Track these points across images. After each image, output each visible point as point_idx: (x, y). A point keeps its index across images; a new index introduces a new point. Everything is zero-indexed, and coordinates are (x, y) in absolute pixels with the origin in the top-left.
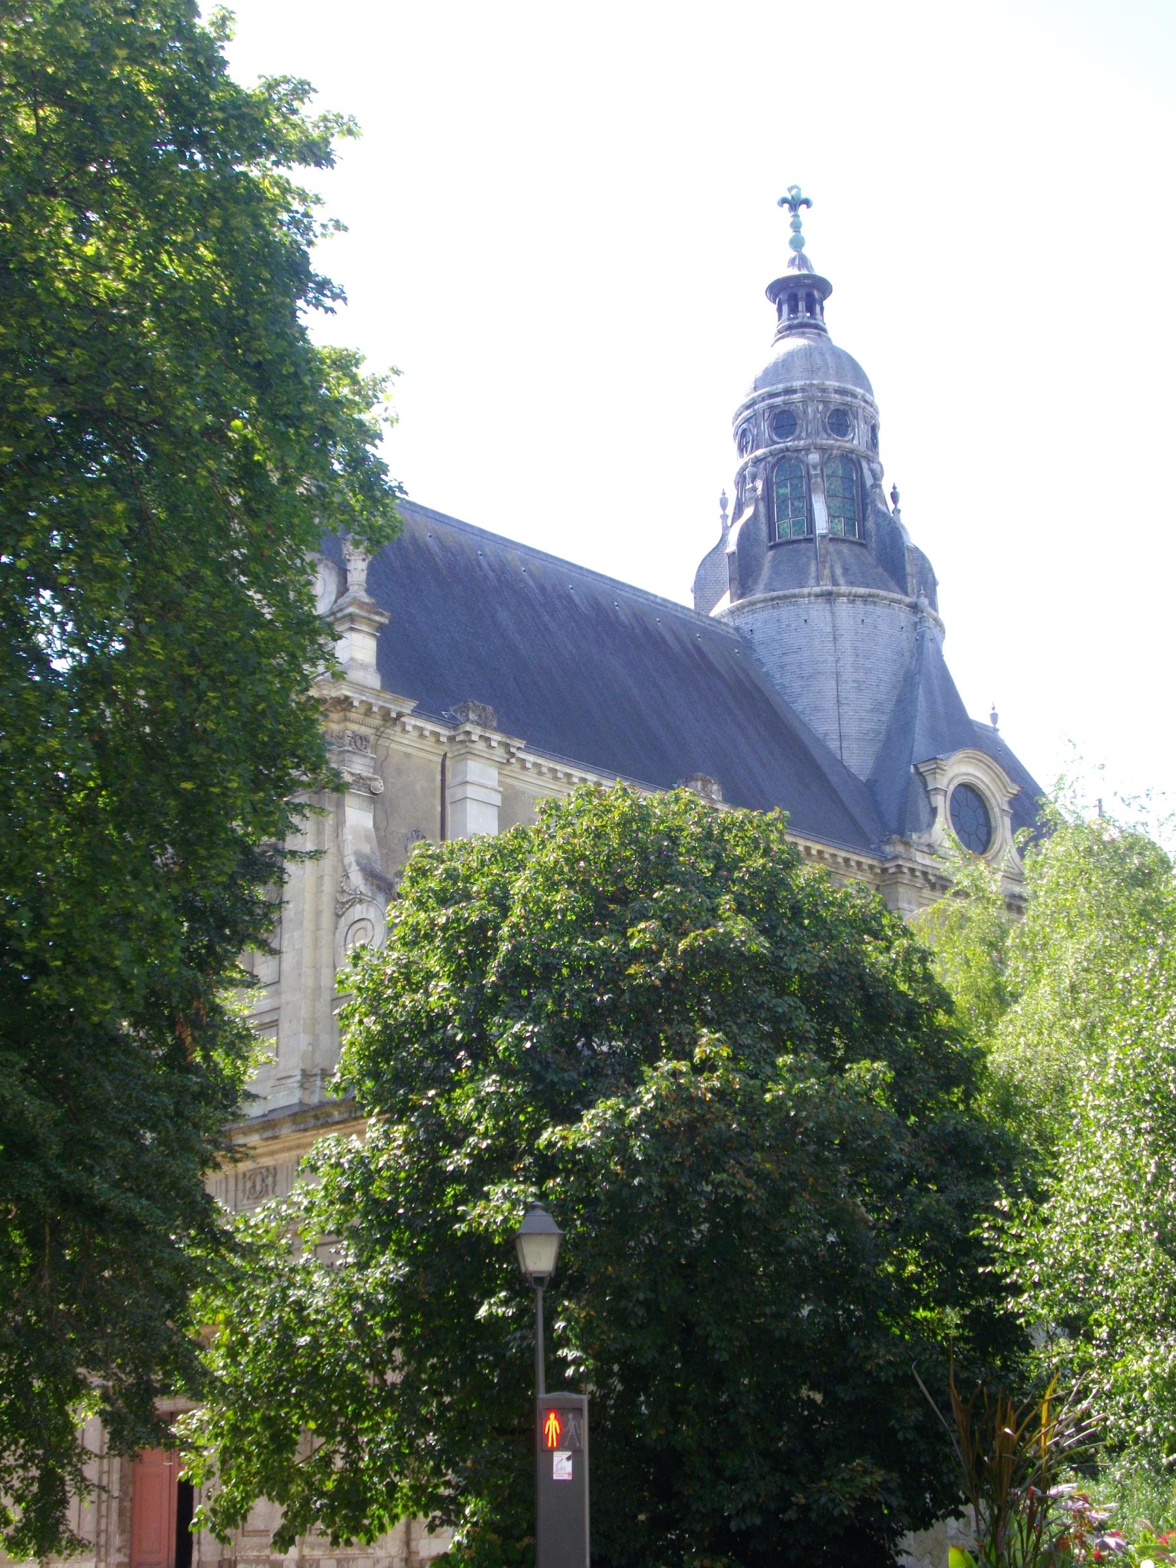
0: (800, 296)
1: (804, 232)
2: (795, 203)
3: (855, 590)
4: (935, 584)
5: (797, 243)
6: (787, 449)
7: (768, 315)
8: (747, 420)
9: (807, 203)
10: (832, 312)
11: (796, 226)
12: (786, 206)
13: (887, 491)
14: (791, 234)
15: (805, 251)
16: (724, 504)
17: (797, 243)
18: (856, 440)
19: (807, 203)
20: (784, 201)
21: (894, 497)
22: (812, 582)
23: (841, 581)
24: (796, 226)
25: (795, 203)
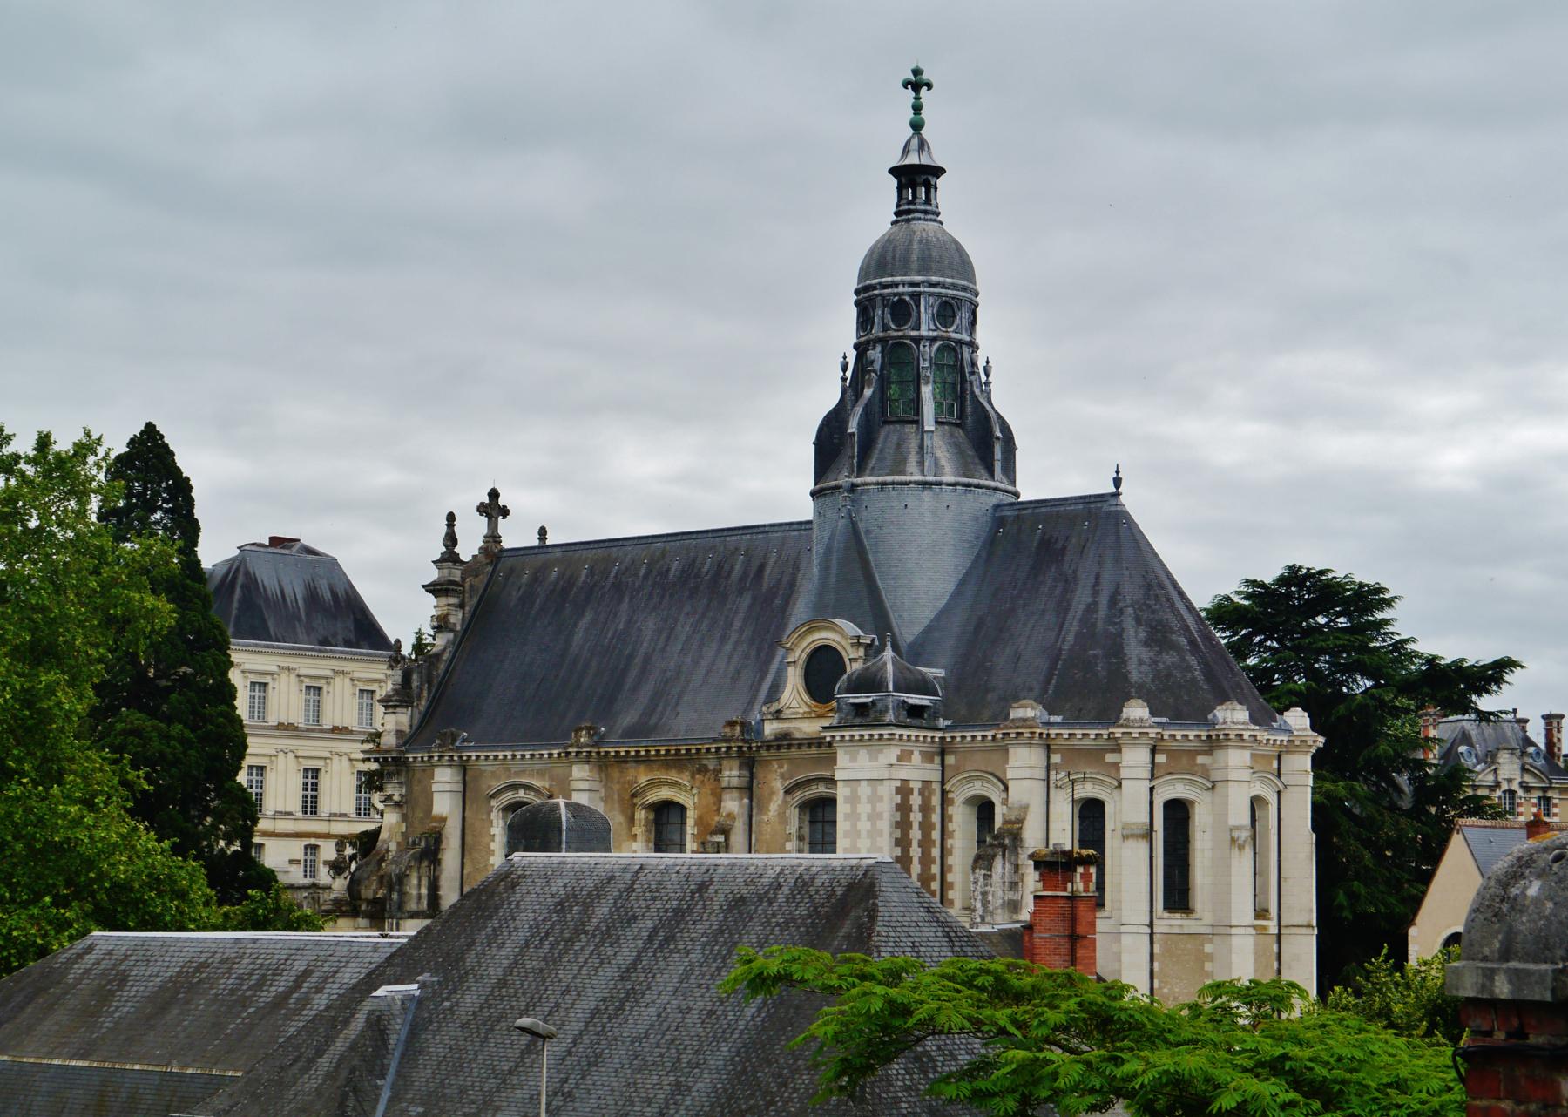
1: (924, 113)
2: (917, 84)
5: (917, 126)
9: (929, 86)
11: (917, 108)
13: (981, 364)
17: (917, 126)
19: (929, 86)
20: (906, 84)
21: (987, 375)
24: (917, 108)
25: (917, 84)
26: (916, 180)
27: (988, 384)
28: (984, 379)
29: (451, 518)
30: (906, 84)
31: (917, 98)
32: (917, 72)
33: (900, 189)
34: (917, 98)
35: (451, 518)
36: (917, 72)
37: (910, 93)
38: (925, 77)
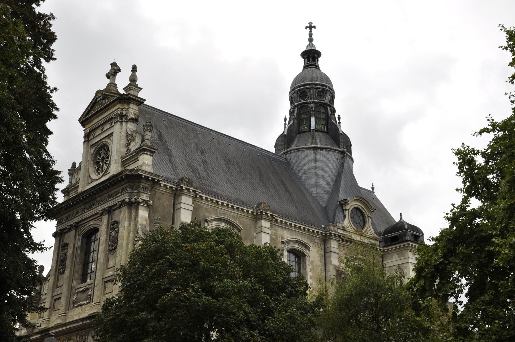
0: (311, 56)
1: (313, 37)
3: (322, 146)
4: (351, 145)
5: (311, 40)
6: (304, 103)
7: (301, 63)
8: (292, 94)
10: (322, 62)
11: (311, 35)
12: (308, 29)
13: (336, 116)
14: (308, 37)
15: (313, 42)
16: (285, 120)
17: (311, 40)
18: (326, 100)
19: (315, 27)
20: (307, 28)
22: (309, 144)
23: (319, 144)
24: (311, 35)
26: (311, 56)
27: (340, 123)
28: (338, 121)
29: (134, 69)
30: (307, 28)
31: (311, 32)
32: (310, 23)
33: (304, 61)
34: (311, 32)
35: (134, 69)
36: (310, 23)
37: (308, 29)
38: (313, 25)
